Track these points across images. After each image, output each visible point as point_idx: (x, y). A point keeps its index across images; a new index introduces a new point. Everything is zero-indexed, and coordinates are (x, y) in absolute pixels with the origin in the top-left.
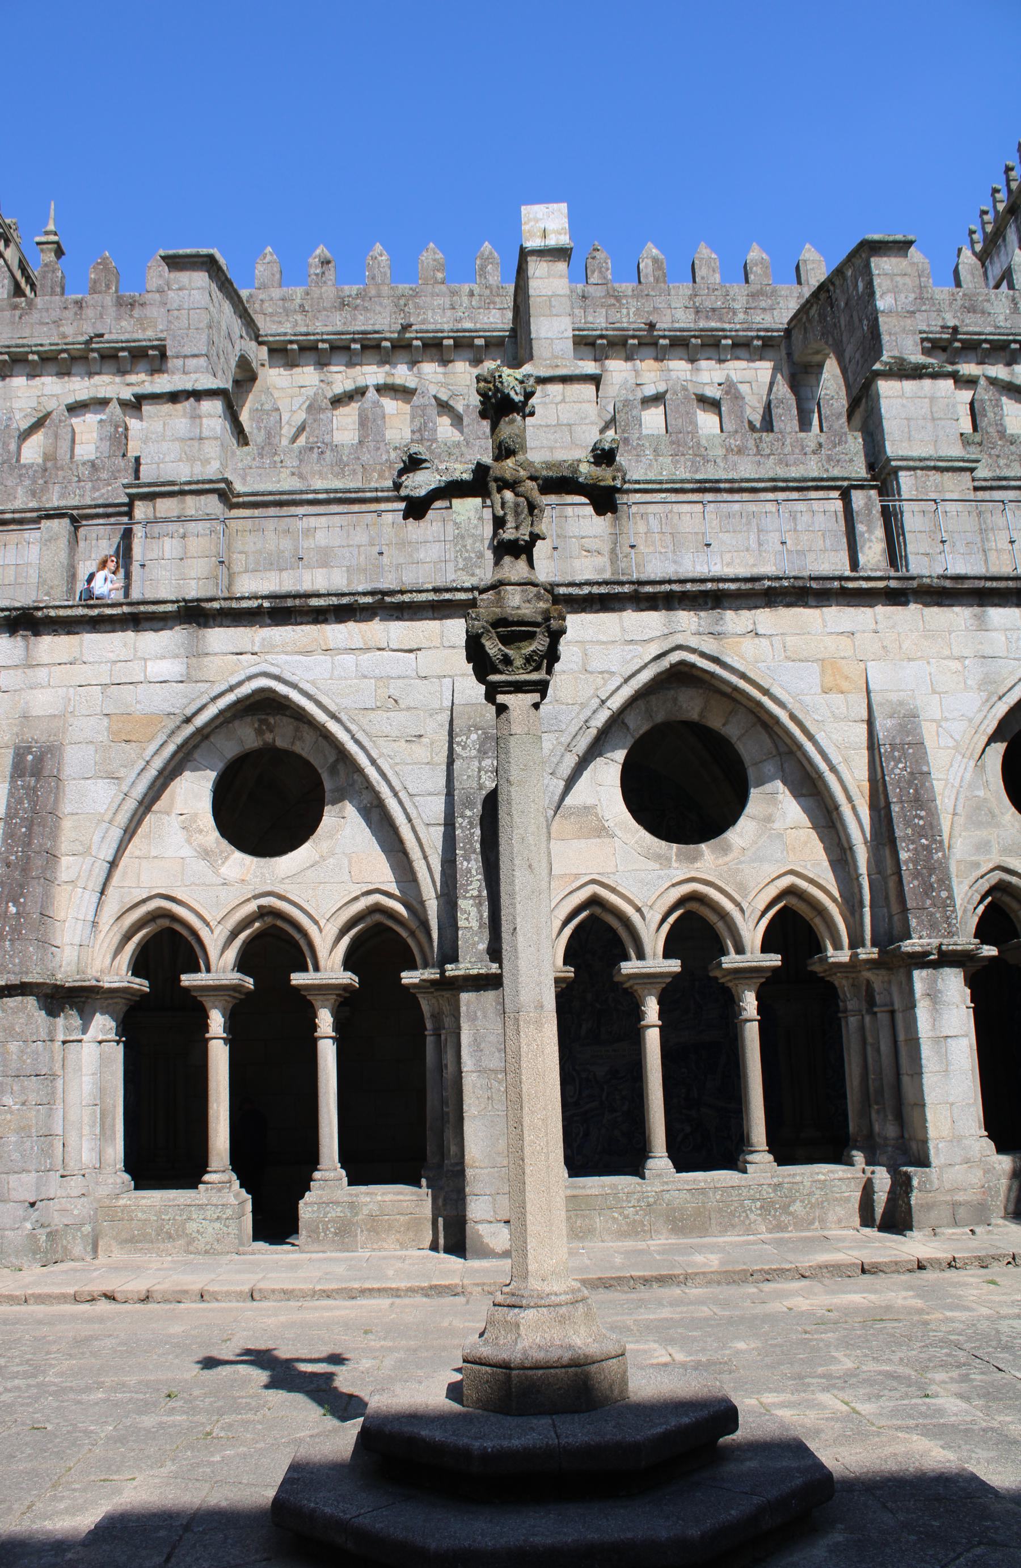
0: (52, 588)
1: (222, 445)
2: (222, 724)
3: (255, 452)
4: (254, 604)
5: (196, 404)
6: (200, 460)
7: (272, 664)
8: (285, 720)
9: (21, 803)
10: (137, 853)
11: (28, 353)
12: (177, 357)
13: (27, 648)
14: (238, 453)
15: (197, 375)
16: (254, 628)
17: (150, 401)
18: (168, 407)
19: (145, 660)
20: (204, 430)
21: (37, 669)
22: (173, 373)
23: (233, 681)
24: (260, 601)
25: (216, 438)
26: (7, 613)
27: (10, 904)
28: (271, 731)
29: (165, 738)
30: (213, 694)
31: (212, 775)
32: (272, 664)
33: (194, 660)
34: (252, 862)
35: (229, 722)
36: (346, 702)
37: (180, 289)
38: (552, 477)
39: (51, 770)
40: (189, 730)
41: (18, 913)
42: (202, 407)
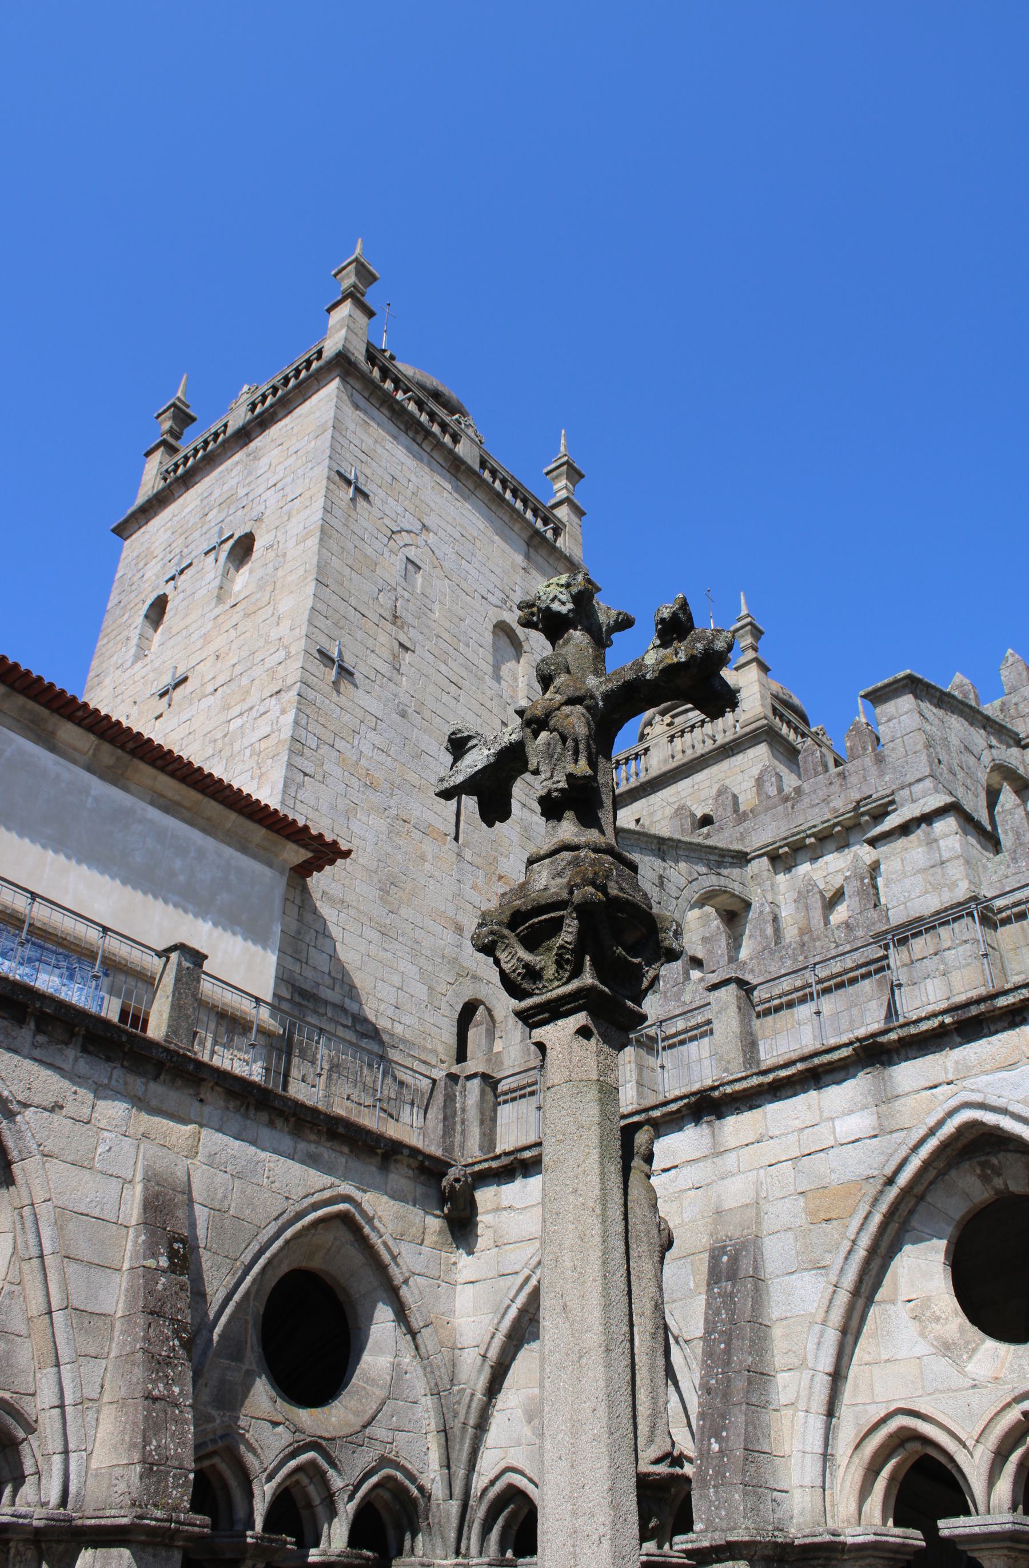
0: (729, 1062)
1: (967, 862)
2: (936, 1178)
3: (1008, 858)
4: (934, 1023)
5: (928, 829)
6: (946, 885)
7: (972, 1091)
8: (1011, 1157)
9: (719, 1314)
10: (867, 1358)
11: (804, 838)
12: (902, 788)
13: (713, 1135)
14: (990, 865)
15: (925, 799)
16: (944, 1053)
17: (883, 842)
18: (902, 842)
19: (832, 1119)
20: (943, 853)
21: (725, 1156)
22: (903, 805)
23: (931, 1121)
24: (940, 1018)
25: (958, 857)
26: (686, 1101)
27: (713, 1440)
28: (999, 1175)
29: (867, 1208)
30: (912, 1143)
31: (943, 1244)
32: (972, 1091)
33: (884, 1107)
34: (1008, 1352)
35: (944, 1174)
37: (889, 720)
38: (612, 690)
39: (747, 1270)
40: (893, 1192)
41: (721, 1451)
42: (935, 830)
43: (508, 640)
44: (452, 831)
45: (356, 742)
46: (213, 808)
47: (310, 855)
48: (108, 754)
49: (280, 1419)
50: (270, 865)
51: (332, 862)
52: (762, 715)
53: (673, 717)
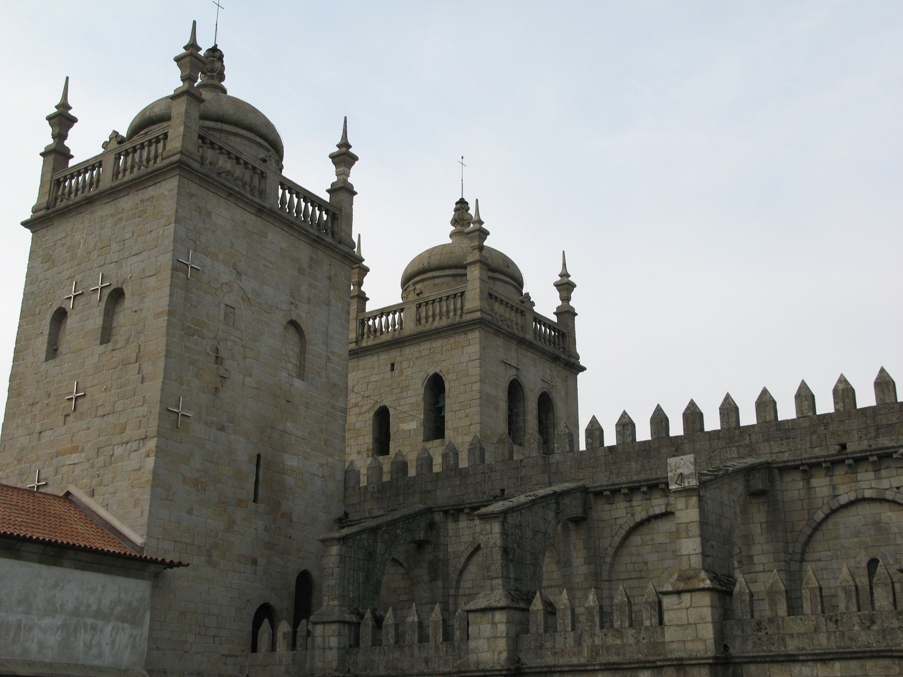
43: (293, 328)
44: (252, 497)
45: (192, 462)
50: (143, 578)
52: (479, 308)
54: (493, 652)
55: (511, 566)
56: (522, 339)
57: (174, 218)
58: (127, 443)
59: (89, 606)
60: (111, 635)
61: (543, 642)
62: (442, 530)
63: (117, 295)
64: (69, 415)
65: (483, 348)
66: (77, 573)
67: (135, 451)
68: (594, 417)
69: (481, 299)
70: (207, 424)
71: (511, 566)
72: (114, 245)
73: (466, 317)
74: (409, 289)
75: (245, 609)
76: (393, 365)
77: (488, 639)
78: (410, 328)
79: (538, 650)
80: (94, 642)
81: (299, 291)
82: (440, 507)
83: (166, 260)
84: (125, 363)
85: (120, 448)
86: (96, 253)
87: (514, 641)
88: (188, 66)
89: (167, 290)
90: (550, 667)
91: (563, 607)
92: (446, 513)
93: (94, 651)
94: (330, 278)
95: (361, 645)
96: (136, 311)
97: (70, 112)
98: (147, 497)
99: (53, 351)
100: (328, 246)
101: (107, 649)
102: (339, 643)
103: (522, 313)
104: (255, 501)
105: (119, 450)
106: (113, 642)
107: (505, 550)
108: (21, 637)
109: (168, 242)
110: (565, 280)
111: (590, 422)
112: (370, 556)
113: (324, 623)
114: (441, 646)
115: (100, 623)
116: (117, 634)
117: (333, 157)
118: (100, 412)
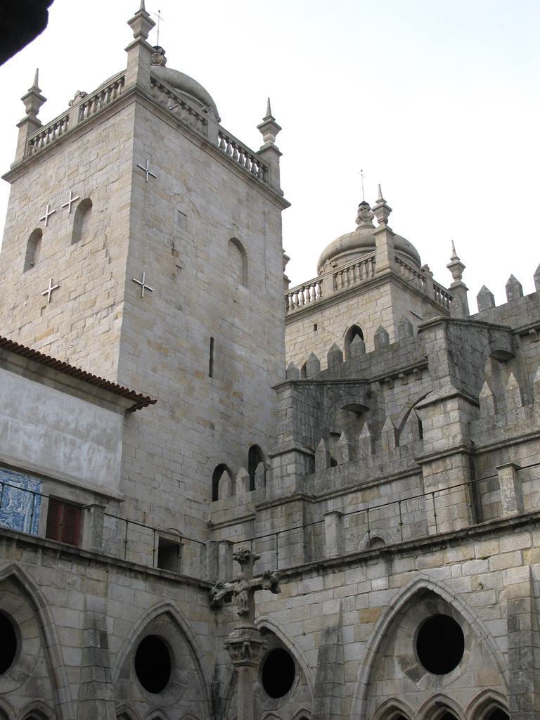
11: (398, 374)
23: (408, 585)
36: (460, 590)
40: (393, 613)
43: (236, 247)
45: (155, 330)
46: (86, 386)
47: (135, 403)
48: (33, 366)
49: (144, 700)
50: (115, 411)
51: (146, 406)
52: (388, 266)
53: (336, 259)
54: (448, 438)
55: (456, 368)
56: (426, 297)
57: (133, 133)
58: (97, 313)
59: (68, 424)
60: (88, 453)
61: (495, 423)
62: (379, 397)
63: (86, 206)
64: (45, 307)
65: (394, 298)
66: (56, 393)
67: (105, 317)
68: (512, 275)
69: (389, 259)
70: (167, 301)
71: (456, 368)
72: (82, 168)
73: (377, 275)
74: (325, 264)
75: (206, 464)
76: (316, 326)
77: (442, 428)
78: (328, 292)
79: (491, 431)
80: (73, 456)
81: (239, 216)
82: (376, 377)
83: (127, 166)
84: (93, 253)
85: (91, 319)
86: (66, 179)
87: (468, 427)
88: (140, 25)
89: (129, 188)
90: (504, 442)
91: (511, 388)
92: (382, 382)
93: (73, 464)
94: (264, 213)
95: (317, 470)
96: (102, 211)
97: (41, 94)
98: (117, 350)
99: (30, 264)
100: (261, 187)
101: (85, 464)
102: (296, 469)
103: (424, 279)
104: (210, 375)
105: (90, 321)
106: (90, 460)
107: (450, 353)
108: (9, 435)
109: (129, 153)
110: (456, 261)
111: (510, 280)
112: (318, 406)
113: (281, 454)
114: (394, 452)
115: (78, 441)
116: (93, 453)
117: (260, 127)
118: (73, 296)
